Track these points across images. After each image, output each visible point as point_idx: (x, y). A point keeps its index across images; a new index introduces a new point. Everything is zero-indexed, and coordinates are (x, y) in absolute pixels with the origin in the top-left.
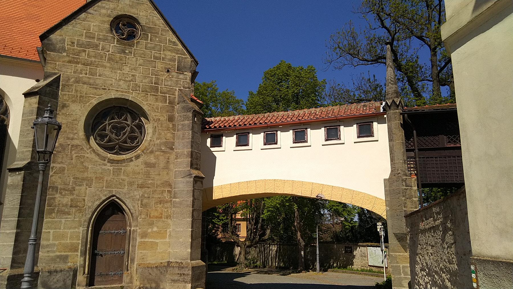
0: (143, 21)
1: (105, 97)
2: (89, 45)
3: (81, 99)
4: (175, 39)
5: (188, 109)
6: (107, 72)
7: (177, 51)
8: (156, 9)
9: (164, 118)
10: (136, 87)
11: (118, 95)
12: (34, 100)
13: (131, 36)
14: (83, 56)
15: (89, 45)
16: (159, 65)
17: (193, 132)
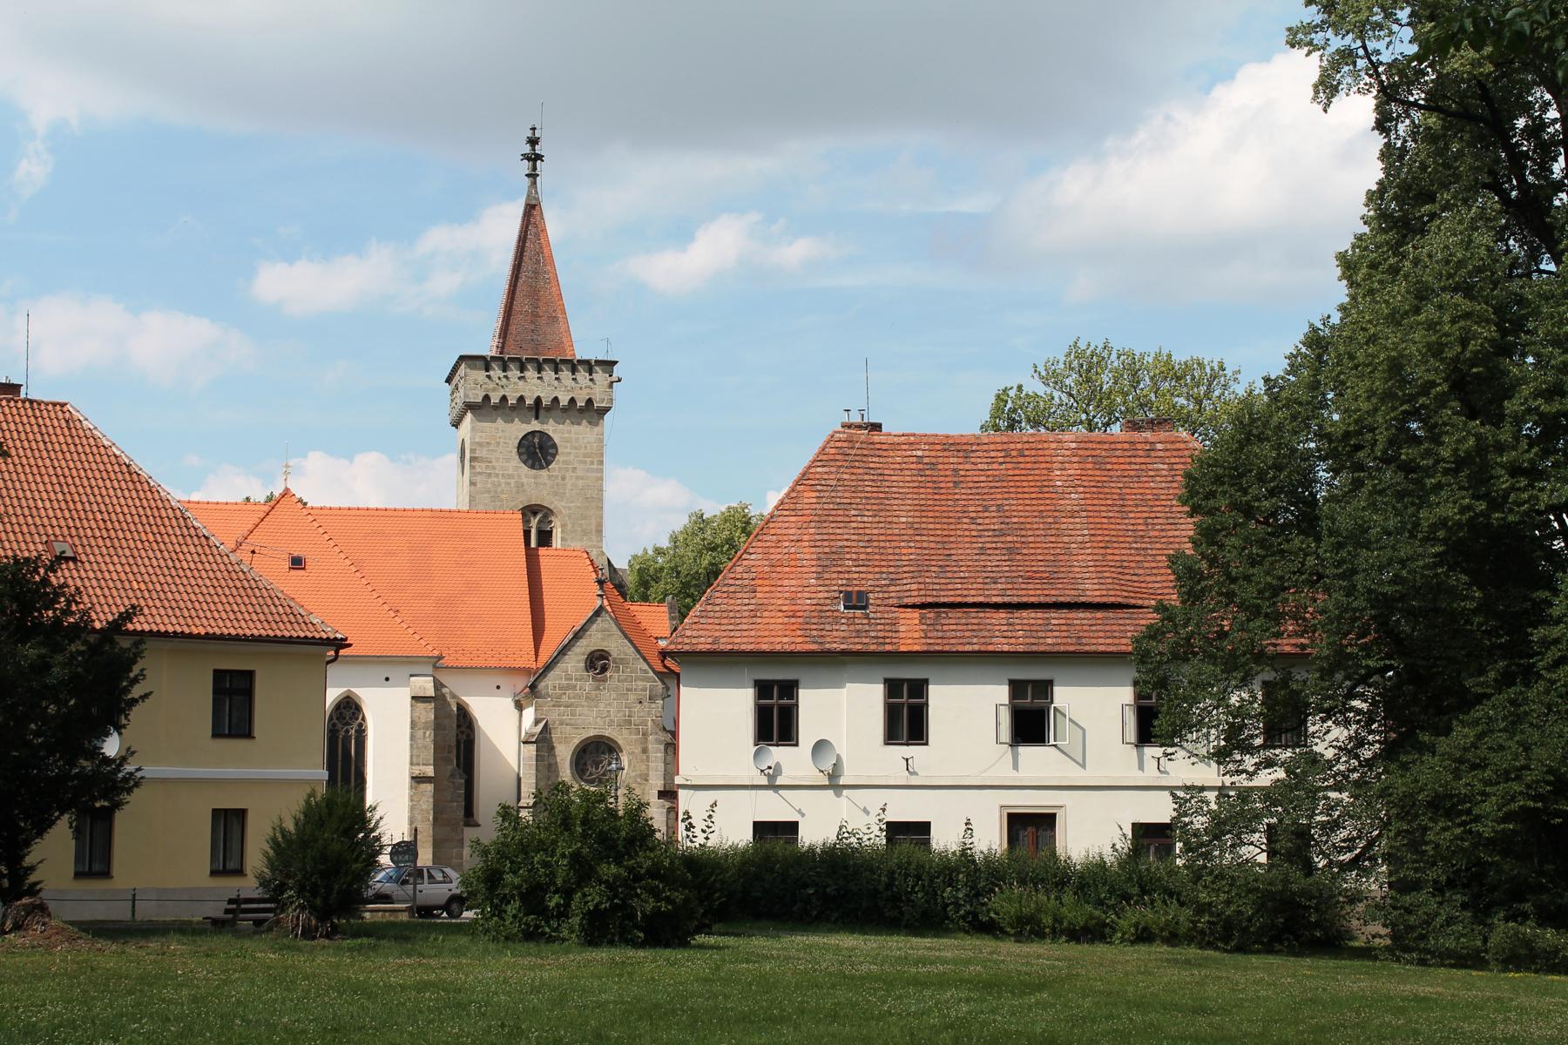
0: (614, 654)
1: (585, 736)
2: (568, 687)
3: (566, 740)
4: (646, 667)
5: (660, 742)
6: (585, 710)
7: (648, 680)
8: (626, 637)
9: (638, 750)
10: (611, 724)
11: (596, 732)
12: (533, 748)
13: (604, 669)
14: (565, 699)
15: (568, 687)
16: (632, 697)
17: (666, 764)
